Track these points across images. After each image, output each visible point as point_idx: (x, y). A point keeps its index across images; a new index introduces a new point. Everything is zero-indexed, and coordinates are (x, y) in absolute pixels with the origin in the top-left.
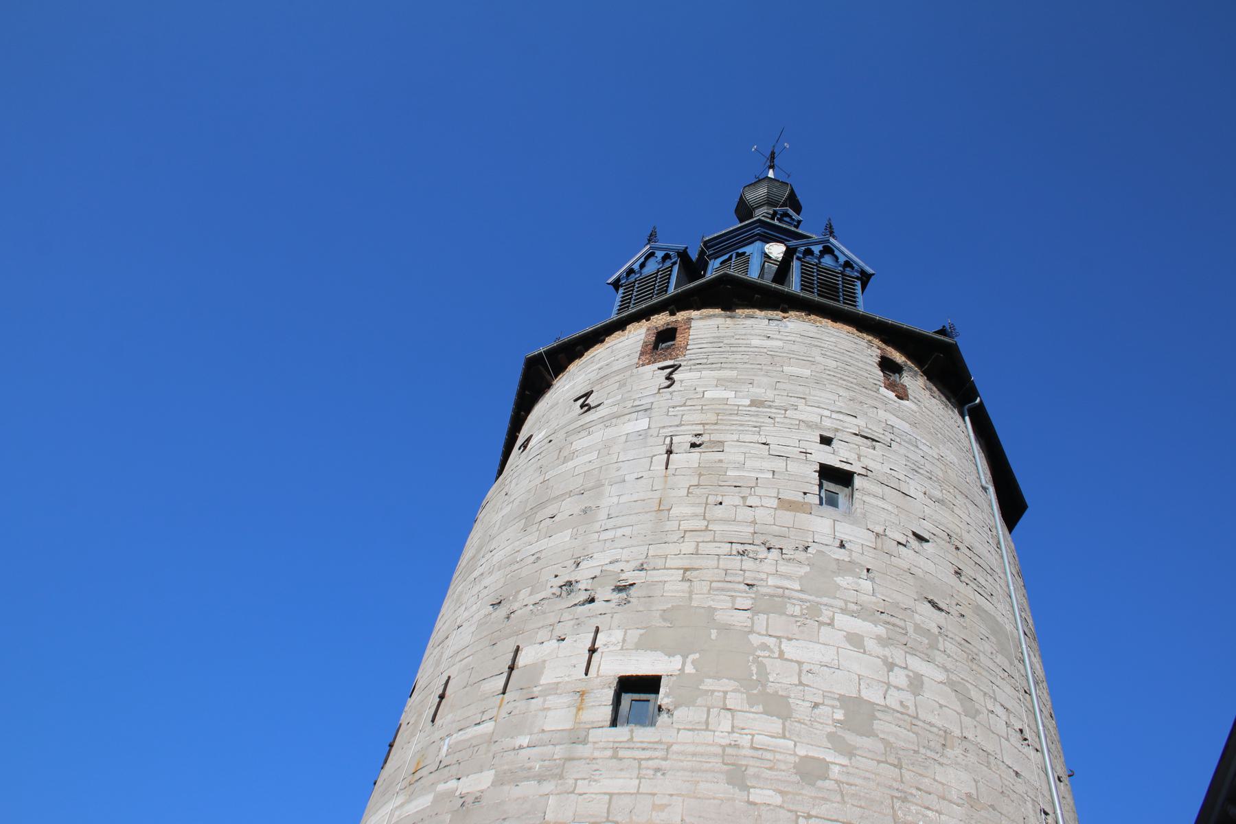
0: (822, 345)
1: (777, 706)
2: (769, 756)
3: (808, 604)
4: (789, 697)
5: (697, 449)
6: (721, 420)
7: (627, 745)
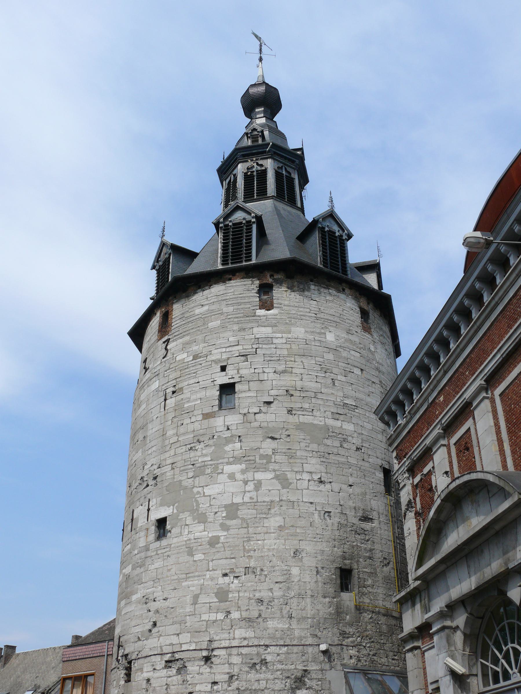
1: (202, 519)
2: (199, 540)
3: (213, 466)
4: (206, 513)
5: (175, 395)
6: (182, 373)
7: (159, 548)
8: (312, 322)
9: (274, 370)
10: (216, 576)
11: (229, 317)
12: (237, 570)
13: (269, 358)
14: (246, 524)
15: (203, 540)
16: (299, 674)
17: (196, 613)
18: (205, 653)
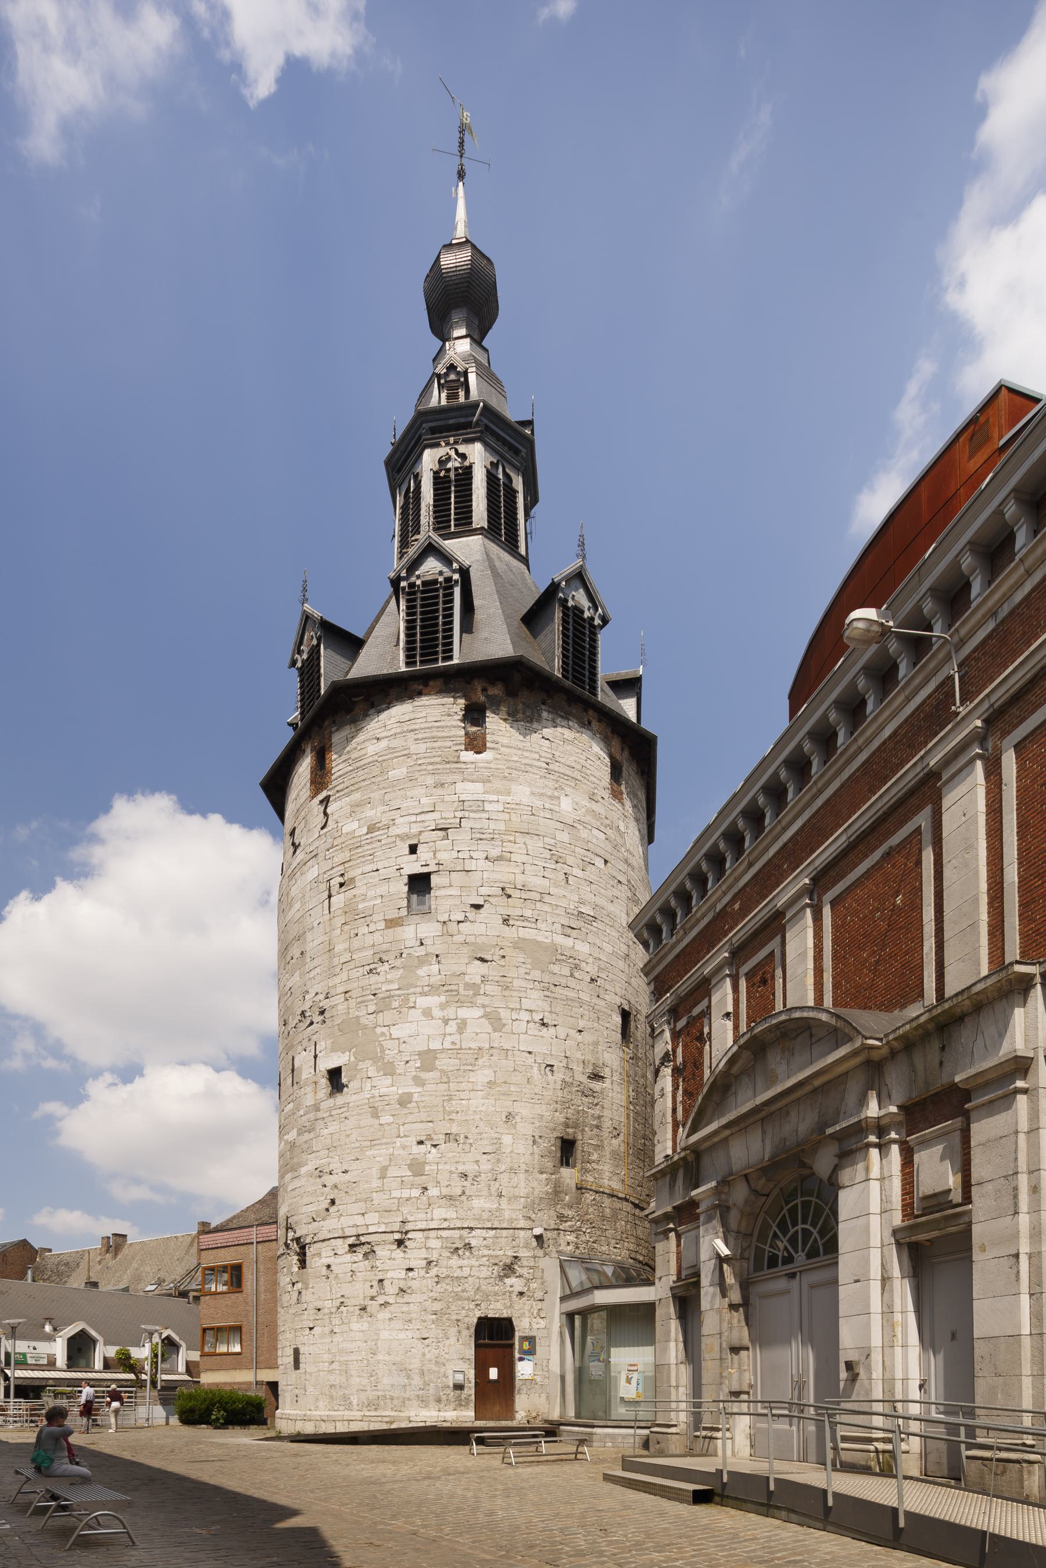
0: (417, 727)
1: (389, 1070)
2: (386, 1098)
8: (541, 777)
9: (485, 856)
10: (408, 1144)
11: (420, 762)
12: (435, 1137)
13: (479, 836)
14: (446, 1078)
15: (391, 1097)
16: (508, 1261)
17: (385, 1188)
18: (397, 1236)
